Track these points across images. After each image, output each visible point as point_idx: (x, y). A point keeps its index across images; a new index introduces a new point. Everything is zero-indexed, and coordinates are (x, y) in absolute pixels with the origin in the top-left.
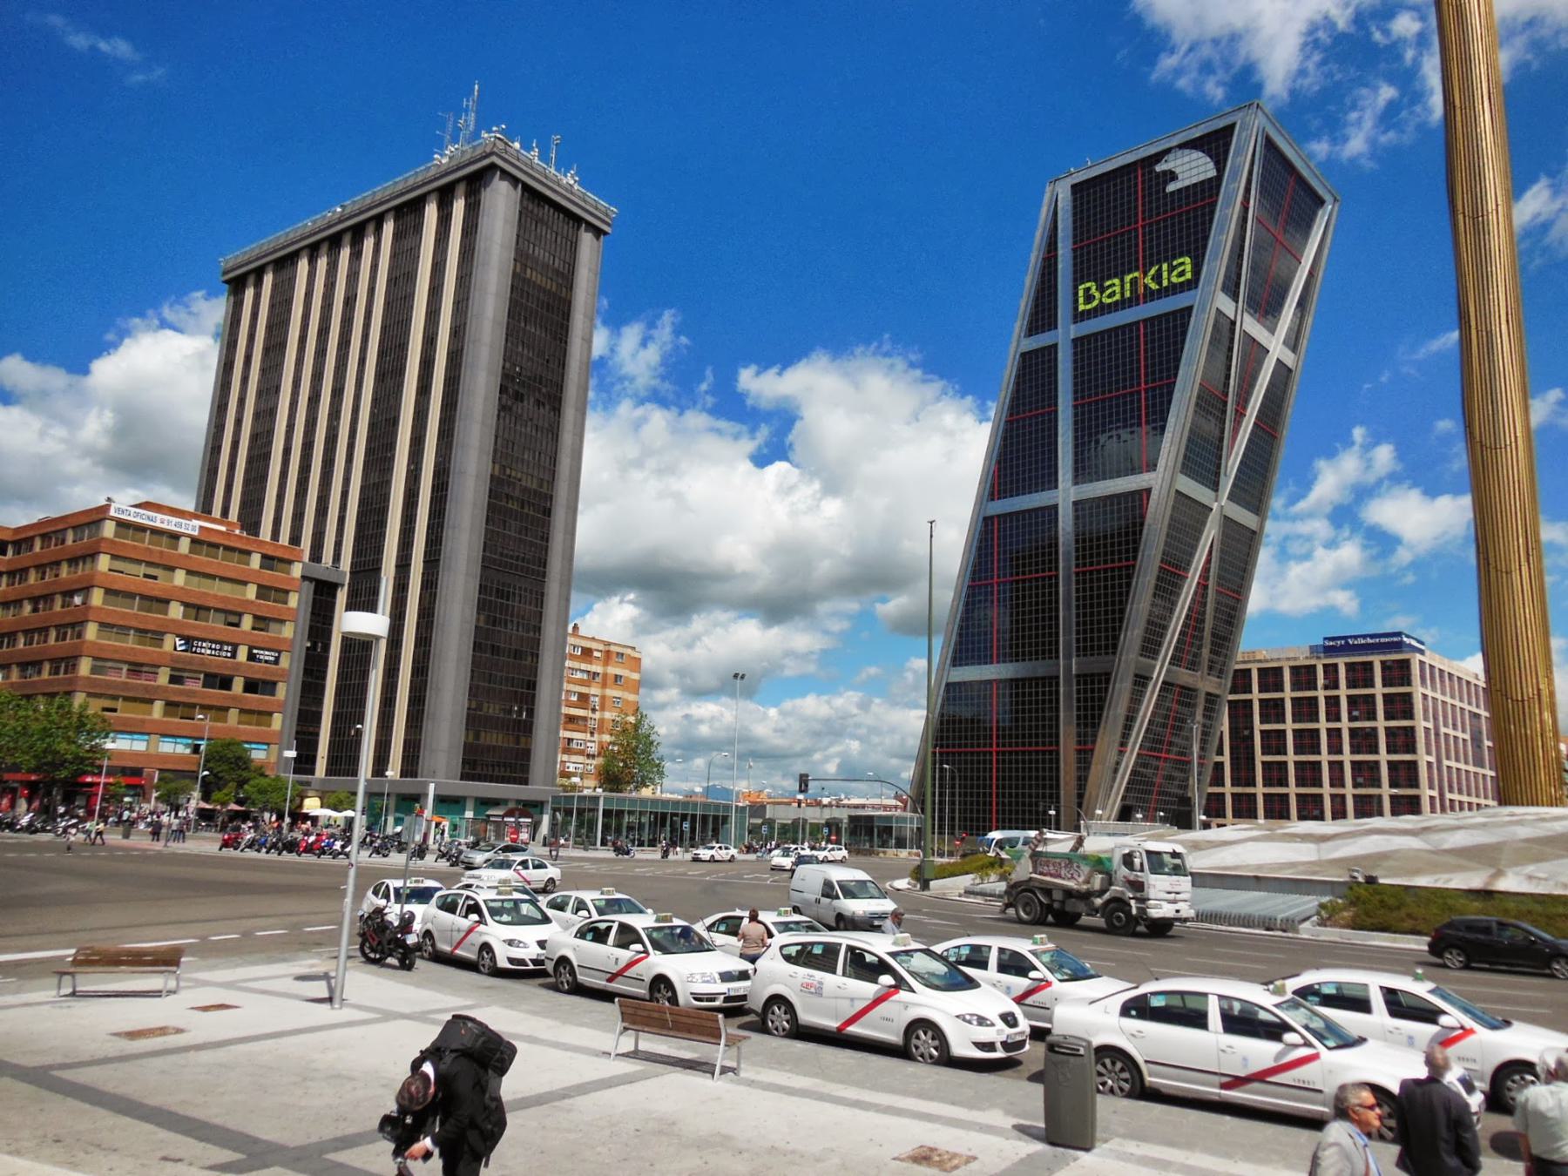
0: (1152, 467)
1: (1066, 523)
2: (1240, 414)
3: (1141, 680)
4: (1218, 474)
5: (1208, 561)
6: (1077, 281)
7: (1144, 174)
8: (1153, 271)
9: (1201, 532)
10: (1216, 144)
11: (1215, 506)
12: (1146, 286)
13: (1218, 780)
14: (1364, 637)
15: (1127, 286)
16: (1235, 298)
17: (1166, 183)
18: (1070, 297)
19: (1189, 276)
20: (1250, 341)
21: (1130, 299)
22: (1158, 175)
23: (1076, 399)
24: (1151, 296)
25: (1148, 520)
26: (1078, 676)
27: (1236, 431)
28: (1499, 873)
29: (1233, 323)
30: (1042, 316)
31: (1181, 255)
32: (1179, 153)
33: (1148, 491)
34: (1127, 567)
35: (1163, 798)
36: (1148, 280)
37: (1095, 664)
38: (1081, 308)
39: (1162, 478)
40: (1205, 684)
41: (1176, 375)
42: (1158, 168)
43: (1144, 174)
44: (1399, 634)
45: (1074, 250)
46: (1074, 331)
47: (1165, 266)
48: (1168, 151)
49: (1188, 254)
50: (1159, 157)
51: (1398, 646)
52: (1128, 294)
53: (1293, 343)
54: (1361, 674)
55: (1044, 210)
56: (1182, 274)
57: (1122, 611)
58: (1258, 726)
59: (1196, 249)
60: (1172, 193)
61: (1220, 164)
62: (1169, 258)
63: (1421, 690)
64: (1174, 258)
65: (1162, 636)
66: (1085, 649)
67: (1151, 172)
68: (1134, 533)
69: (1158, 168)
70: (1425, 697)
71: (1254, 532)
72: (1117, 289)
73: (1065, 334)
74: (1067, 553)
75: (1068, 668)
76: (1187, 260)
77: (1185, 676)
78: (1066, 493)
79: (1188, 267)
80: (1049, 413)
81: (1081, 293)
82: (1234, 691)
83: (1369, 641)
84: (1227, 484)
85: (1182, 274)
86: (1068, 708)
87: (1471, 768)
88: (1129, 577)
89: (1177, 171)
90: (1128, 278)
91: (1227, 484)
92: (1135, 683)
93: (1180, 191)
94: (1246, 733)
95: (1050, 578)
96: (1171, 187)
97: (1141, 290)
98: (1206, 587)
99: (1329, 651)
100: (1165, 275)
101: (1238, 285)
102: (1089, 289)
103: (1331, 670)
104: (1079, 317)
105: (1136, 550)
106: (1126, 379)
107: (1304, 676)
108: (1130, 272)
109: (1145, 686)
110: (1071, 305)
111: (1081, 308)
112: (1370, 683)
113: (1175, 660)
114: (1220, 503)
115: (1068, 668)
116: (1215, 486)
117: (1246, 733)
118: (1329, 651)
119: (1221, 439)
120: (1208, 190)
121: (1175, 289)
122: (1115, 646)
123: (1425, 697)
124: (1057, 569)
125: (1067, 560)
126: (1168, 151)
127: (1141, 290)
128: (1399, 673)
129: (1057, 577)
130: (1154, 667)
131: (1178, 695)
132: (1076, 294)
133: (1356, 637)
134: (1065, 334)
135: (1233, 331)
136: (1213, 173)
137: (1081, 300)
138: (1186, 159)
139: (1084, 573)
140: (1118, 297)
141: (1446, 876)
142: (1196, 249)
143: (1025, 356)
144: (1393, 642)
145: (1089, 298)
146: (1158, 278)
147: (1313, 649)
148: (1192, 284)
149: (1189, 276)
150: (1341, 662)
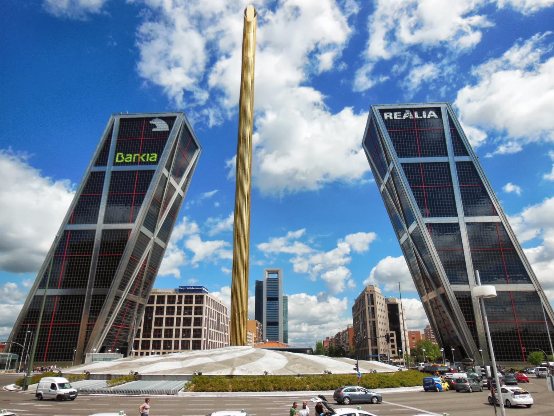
0: (133, 221)
1: (98, 237)
2: (165, 209)
3: (117, 298)
4: (154, 227)
5: (147, 257)
6: (117, 152)
8: (144, 155)
9: (146, 246)
10: (170, 120)
11: (152, 238)
12: (141, 160)
13: (138, 336)
14: (192, 287)
15: (134, 158)
16: (169, 170)
17: (152, 128)
18: (113, 157)
19: (155, 160)
20: (171, 186)
21: (135, 163)
22: (150, 124)
23: (109, 193)
24: (142, 163)
25: (129, 240)
26: (93, 295)
27: (162, 214)
28: (234, 369)
29: (167, 179)
30: (102, 160)
31: (154, 152)
32: (158, 120)
33: (131, 230)
34: (119, 256)
35: (119, 345)
36: (142, 158)
37: (100, 291)
38: (117, 161)
39: (135, 227)
40: (139, 300)
41: (146, 192)
42: (151, 122)
43: (145, 123)
44: (201, 287)
45: (118, 141)
46: (113, 168)
47: (148, 155)
48: (154, 118)
49: (156, 153)
51: (201, 291)
52: (134, 161)
53: (184, 189)
54: (189, 300)
55: (109, 124)
56: (153, 159)
57: (114, 272)
58: (154, 316)
59: (159, 152)
61: (170, 127)
62: (150, 152)
63: (206, 305)
64: (152, 153)
65: (127, 282)
66: (98, 285)
67: (148, 123)
68: (123, 244)
69: (151, 122)
70: (206, 308)
71: (163, 249)
72: (131, 158)
73: (109, 169)
74: (97, 248)
75: (90, 292)
76: (156, 155)
77: (132, 297)
78: (100, 226)
79: (156, 157)
80: (98, 196)
81: (118, 156)
82: (148, 303)
84: (157, 231)
85: (153, 159)
86: (87, 308)
87: (216, 331)
88: (119, 260)
89: (157, 125)
90: (135, 155)
91: (157, 231)
92: (115, 299)
93: (157, 132)
94: (150, 318)
95: (88, 257)
96: (154, 130)
97: (139, 161)
98: (145, 266)
100: (148, 157)
101: (170, 167)
102: (120, 156)
104: (115, 164)
105: (123, 250)
106: (130, 189)
107: (171, 299)
108: (136, 153)
109: (118, 300)
110: (113, 160)
111: (117, 161)
112: (191, 303)
113: (131, 292)
114: (154, 238)
115: (90, 292)
117: (150, 318)
118: (181, 291)
119: (157, 216)
120: (165, 135)
121: (150, 163)
122: (109, 285)
123: (206, 308)
124: (91, 254)
125: (96, 251)
126: (154, 118)
127: (139, 161)
128: (200, 299)
129: (91, 257)
130: (122, 293)
131: (130, 304)
132: (115, 156)
133: (189, 287)
134: (109, 169)
135: (166, 181)
136: (167, 129)
137: (117, 158)
138: (160, 122)
139: (102, 256)
140: (130, 161)
141: (220, 371)
142: (159, 152)
143: (93, 174)
144: (199, 290)
145: (120, 158)
146: (145, 158)
147: (176, 290)
148: (156, 163)
149: (155, 160)
150: (184, 295)
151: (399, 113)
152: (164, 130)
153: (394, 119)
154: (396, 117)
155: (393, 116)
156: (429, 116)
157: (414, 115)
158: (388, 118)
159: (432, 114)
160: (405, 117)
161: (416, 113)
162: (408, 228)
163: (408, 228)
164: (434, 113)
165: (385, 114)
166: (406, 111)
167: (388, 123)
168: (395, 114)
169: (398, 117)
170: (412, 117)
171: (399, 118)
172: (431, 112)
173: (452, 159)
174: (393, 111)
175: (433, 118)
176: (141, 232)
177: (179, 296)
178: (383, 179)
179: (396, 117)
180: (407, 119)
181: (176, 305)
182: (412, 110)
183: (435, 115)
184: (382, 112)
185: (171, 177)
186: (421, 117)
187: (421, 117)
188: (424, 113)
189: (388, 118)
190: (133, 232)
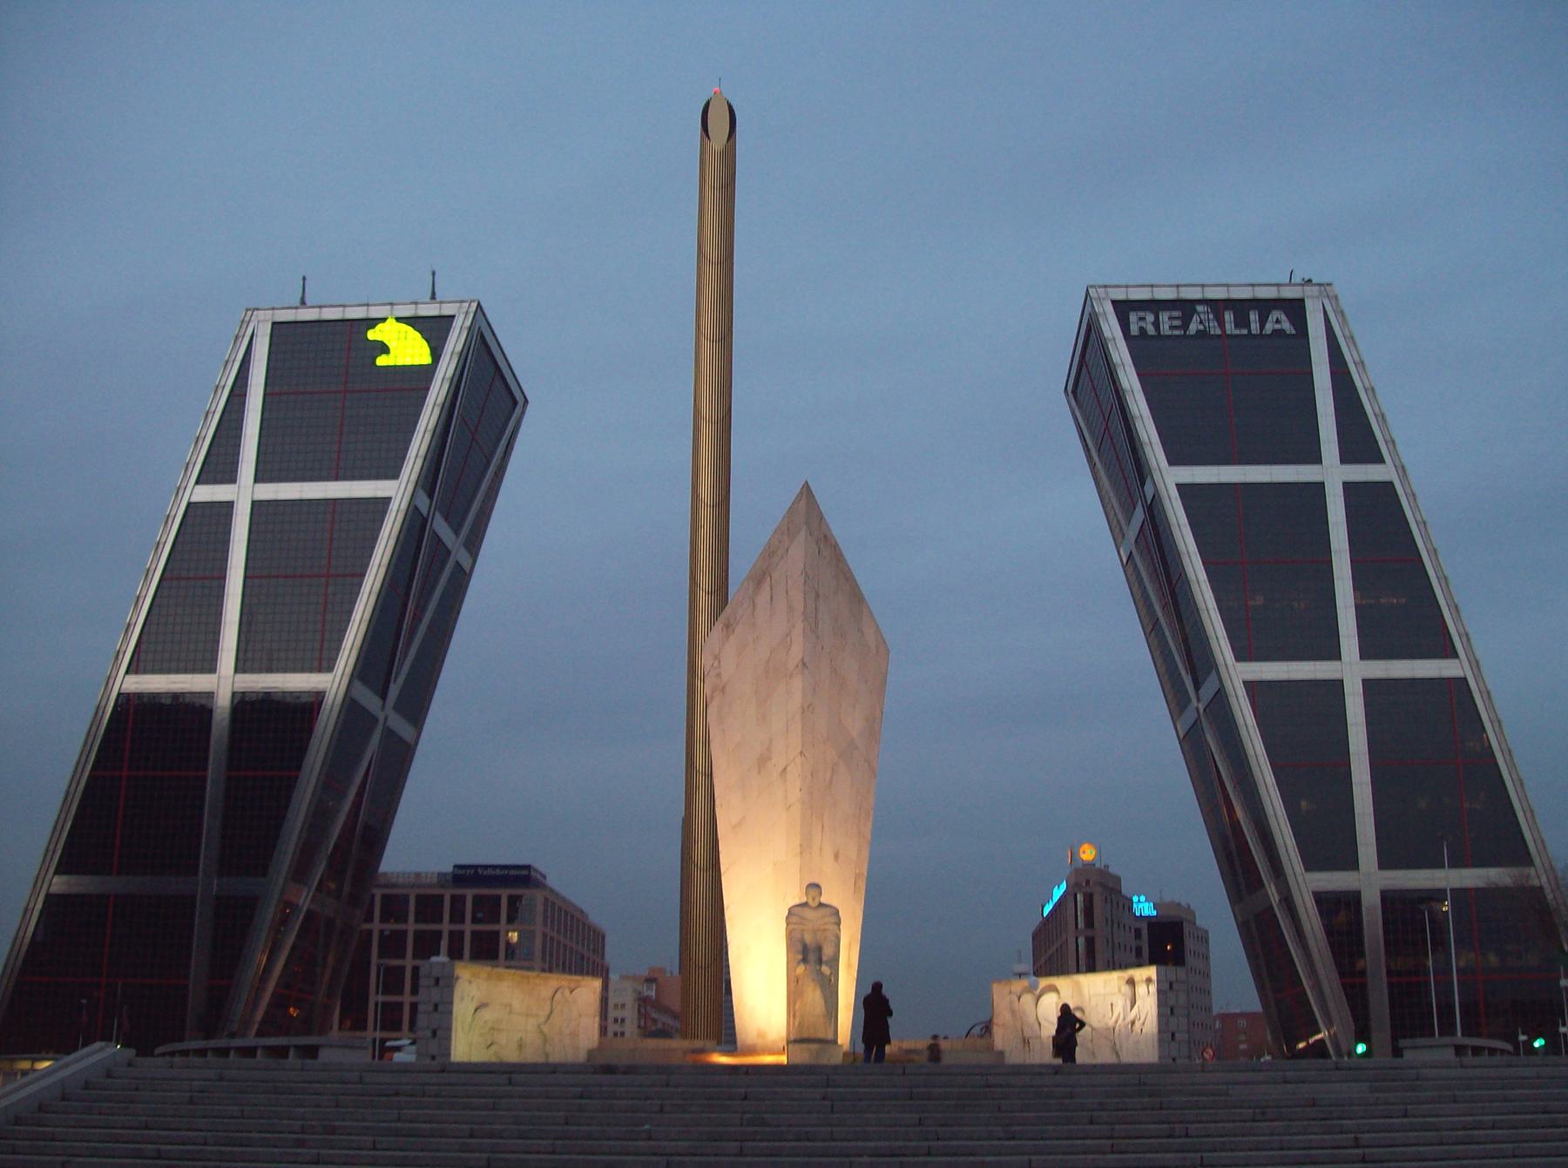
0: (325, 665)
7: (350, 339)
10: (433, 329)
16: (431, 496)
20: (438, 540)
29: (425, 520)
30: (220, 466)
42: (372, 335)
44: (528, 867)
50: (373, 322)
54: (488, 909)
69: (372, 335)
73: (244, 492)
83: (498, 872)
91: (394, 691)
96: (382, 361)
103: (458, 901)
107: (429, 906)
116: (384, 697)
120: (418, 378)
123: (545, 935)
134: (244, 492)
150: (470, 893)
151: (1176, 314)
153: (1159, 336)
154: (1165, 329)
155: (1156, 324)
156: (1269, 327)
157: (1222, 324)
159: (1278, 321)
160: (1194, 327)
161: (1229, 317)
162: (1197, 685)
163: (1197, 685)
164: (1283, 317)
165: (1133, 317)
166: (1200, 308)
168: (1164, 316)
169: (1171, 327)
170: (1219, 332)
171: (1177, 332)
172: (1275, 315)
173: (1333, 473)
175: (1278, 333)
176: (354, 701)
177: (453, 897)
178: (1129, 522)
179: (1165, 329)
180: (1202, 334)
181: (446, 927)
182: (1218, 307)
183: (1286, 326)
184: (1123, 308)
185: (438, 515)
186: (1245, 332)
187: (1245, 332)
188: (1254, 316)
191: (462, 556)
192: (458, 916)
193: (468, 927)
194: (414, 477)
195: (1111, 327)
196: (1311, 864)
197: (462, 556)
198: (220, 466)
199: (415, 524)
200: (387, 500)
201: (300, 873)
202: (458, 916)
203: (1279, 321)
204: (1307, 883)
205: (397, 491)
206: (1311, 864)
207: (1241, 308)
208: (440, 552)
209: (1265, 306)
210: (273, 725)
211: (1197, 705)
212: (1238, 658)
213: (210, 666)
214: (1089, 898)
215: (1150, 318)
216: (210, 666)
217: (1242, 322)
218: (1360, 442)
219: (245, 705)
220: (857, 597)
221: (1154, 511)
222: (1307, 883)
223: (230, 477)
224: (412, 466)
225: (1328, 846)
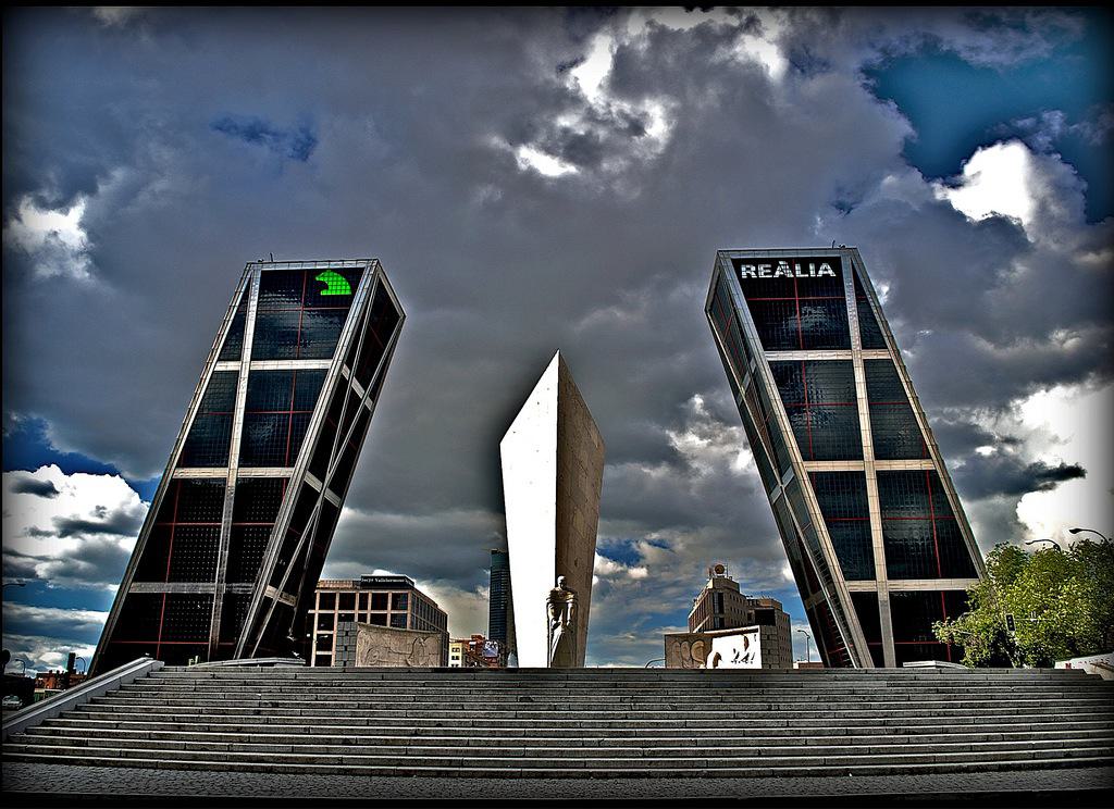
0: (292, 464)
5: (312, 528)
10: (353, 276)
16: (351, 369)
32: (331, 274)
37: (238, 588)
39: (295, 473)
42: (317, 279)
54: (380, 602)
60: (324, 296)
61: (354, 289)
73: (245, 366)
89: (330, 284)
91: (328, 477)
94: (308, 635)
96: (324, 293)
99: (365, 585)
103: (364, 598)
107: (347, 602)
116: (323, 482)
117: (308, 635)
118: (365, 585)
126: (324, 270)
134: (245, 366)
136: (348, 293)
150: (370, 593)
151: (767, 266)
152: (343, 293)
155: (756, 272)
157: (794, 272)
158: (748, 275)
161: (797, 267)
163: (781, 475)
165: (743, 269)
166: (781, 263)
167: (749, 286)
168: (761, 268)
169: (765, 274)
170: (792, 276)
172: (824, 266)
174: (756, 262)
182: (791, 262)
183: (830, 272)
184: (737, 264)
188: (812, 267)
189: (748, 275)
190: (291, 483)
191: (368, 403)
192: (363, 606)
193: (369, 612)
194: (341, 358)
195: (731, 275)
196: (849, 577)
197: (368, 403)
198: (232, 351)
199: (342, 384)
200: (326, 371)
201: (275, 582)
202: (363, 606)
203: (826, 270)
204: (846, 588)
205: (332, 366)
206: (849, 577)
207: (805, 263)
208: (355, 400)
209: (818, 262)
210: (258, 499)
211: (782, 485)
212: (804, 459)
213: (224, 463)
214: (720, 595)
215: (753, 268)
216: (224, 463)
217: (805, 270)
218: (872, 339)
219: (244, 486)
220: (589, 417)
221: (756, 377)
222: (846, 588)
223: (238, 358)
224: (341, 351)
225: (857, 561)
